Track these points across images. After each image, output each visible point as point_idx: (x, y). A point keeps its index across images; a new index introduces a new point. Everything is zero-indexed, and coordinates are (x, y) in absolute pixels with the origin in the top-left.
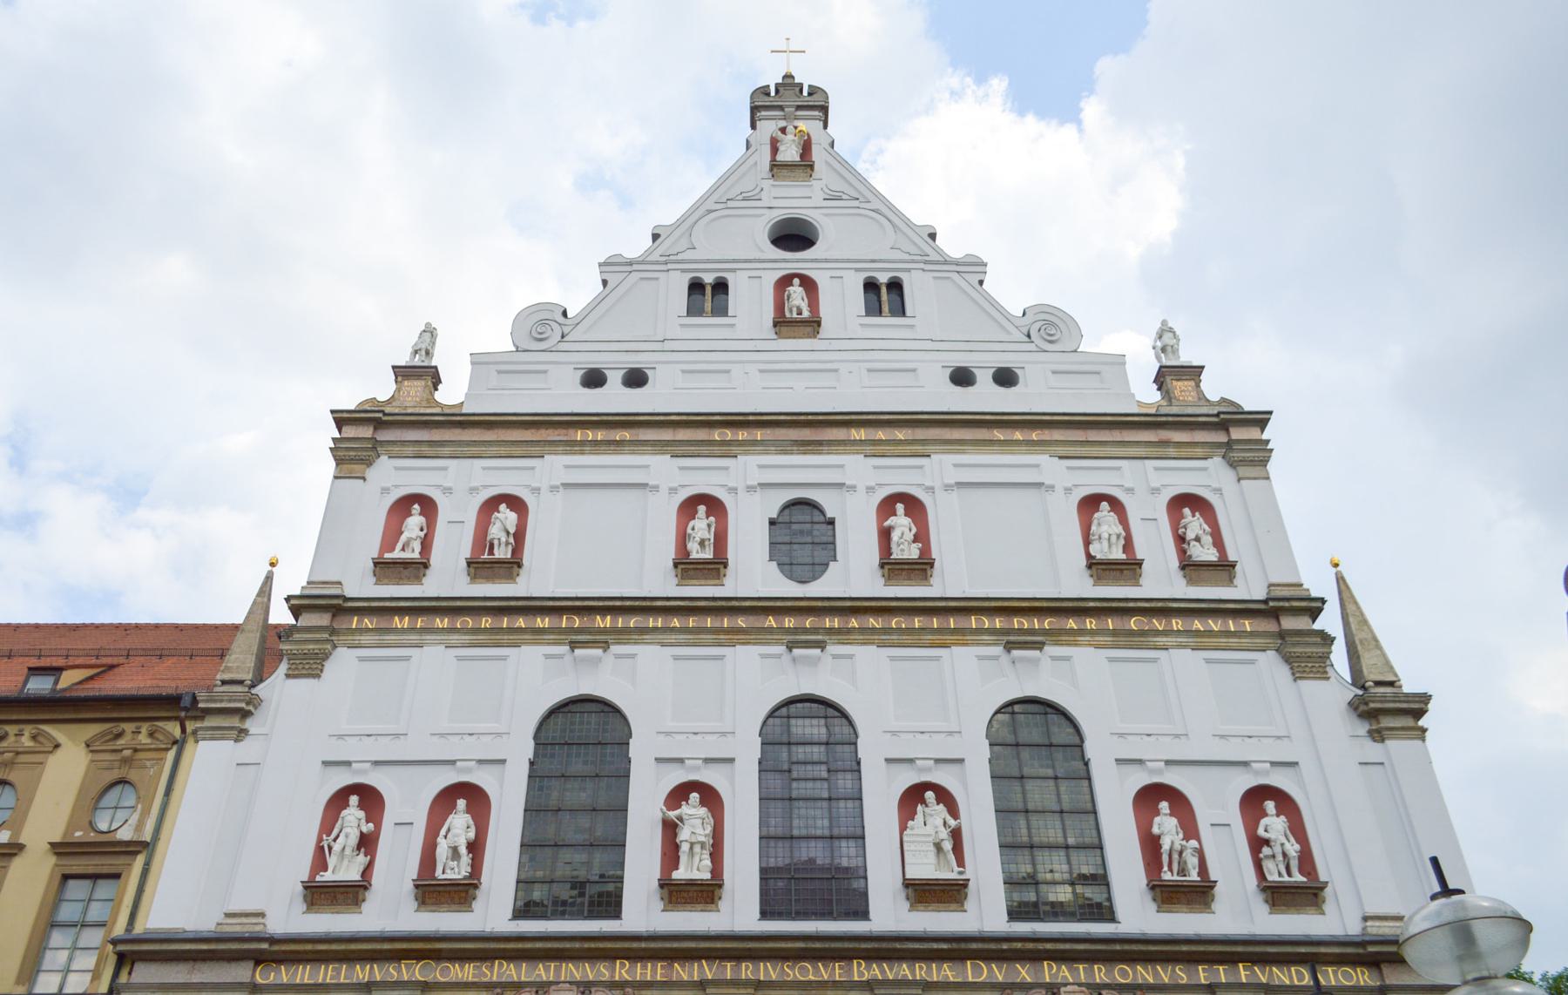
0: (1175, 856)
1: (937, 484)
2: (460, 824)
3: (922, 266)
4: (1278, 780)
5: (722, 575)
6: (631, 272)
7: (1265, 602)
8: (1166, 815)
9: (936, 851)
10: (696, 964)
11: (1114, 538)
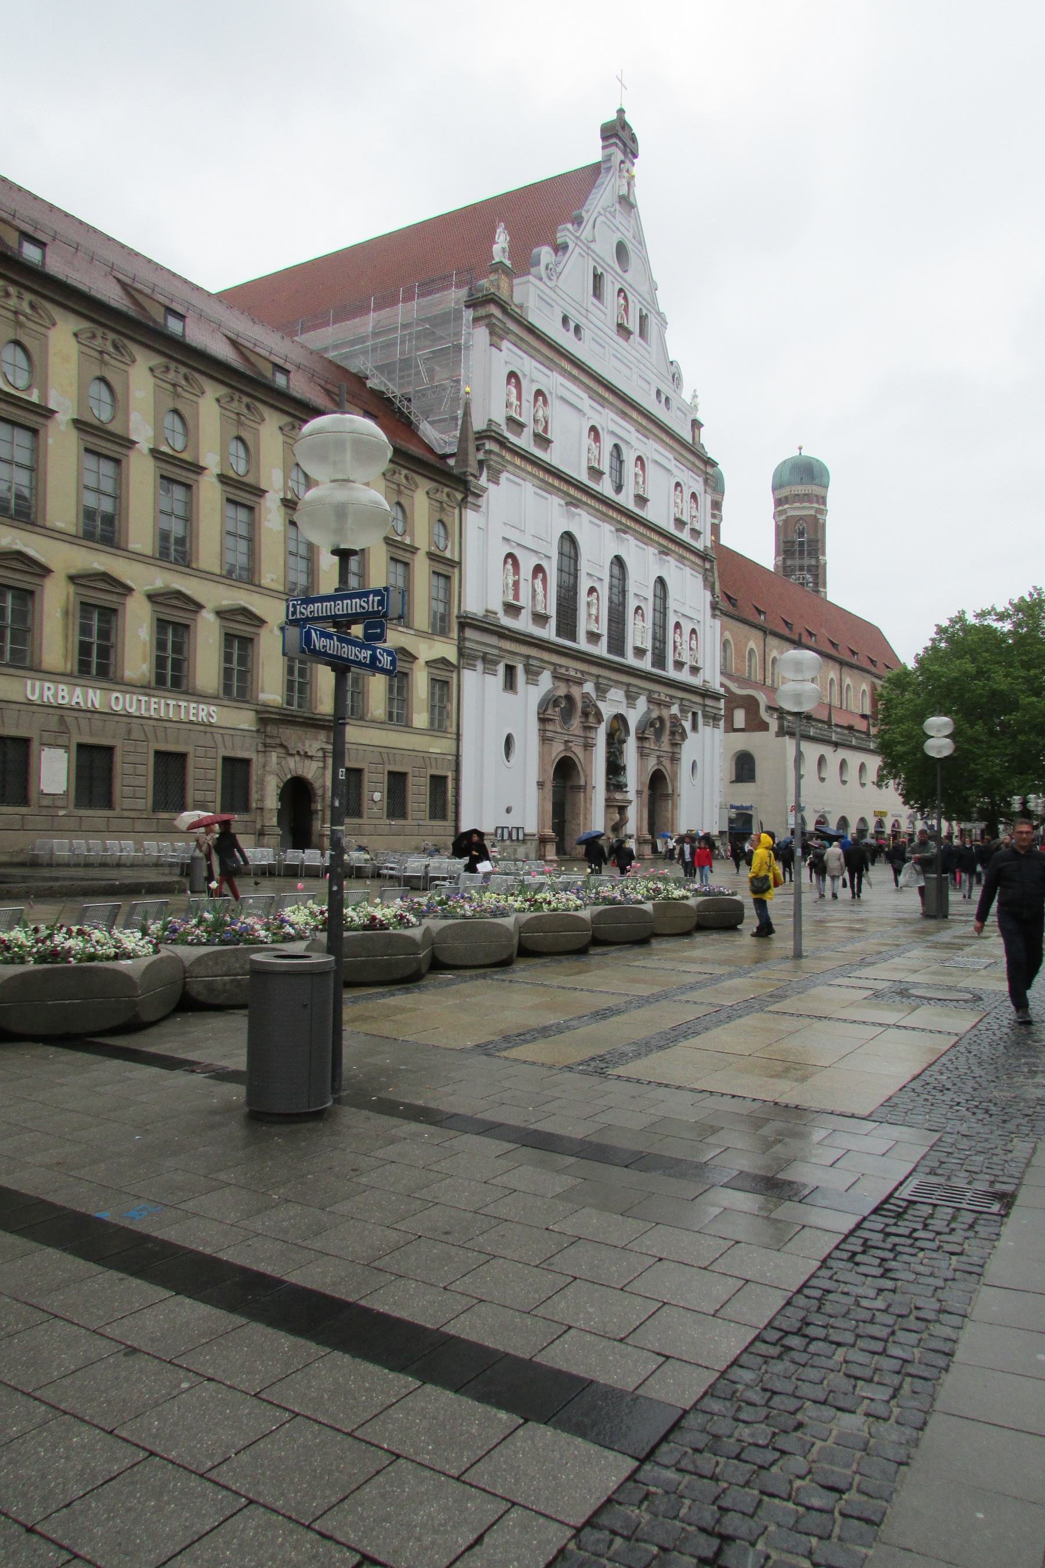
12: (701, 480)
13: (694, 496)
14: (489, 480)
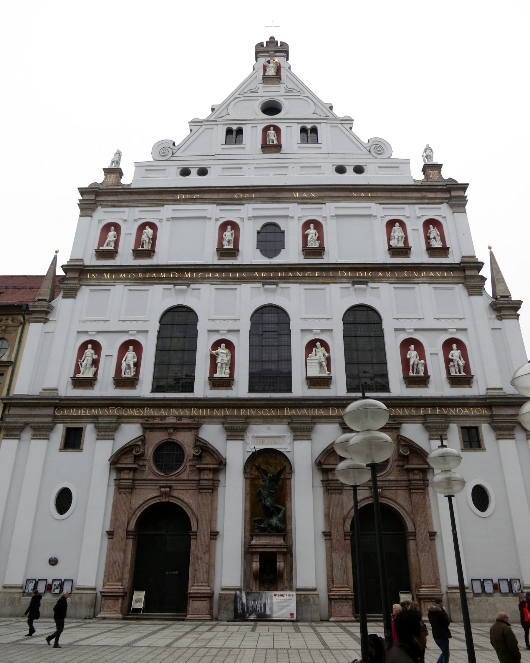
0: (415, 366)
1: (328, 216)
2: (130, 356)
3: (325, 121)
4: (459, 336)
5: (236, 255)
6: (202, 126)
7: (459, 264)
8: (413, 350)
9: (319, 366)
10: (223, 410)
11: (400, 238)
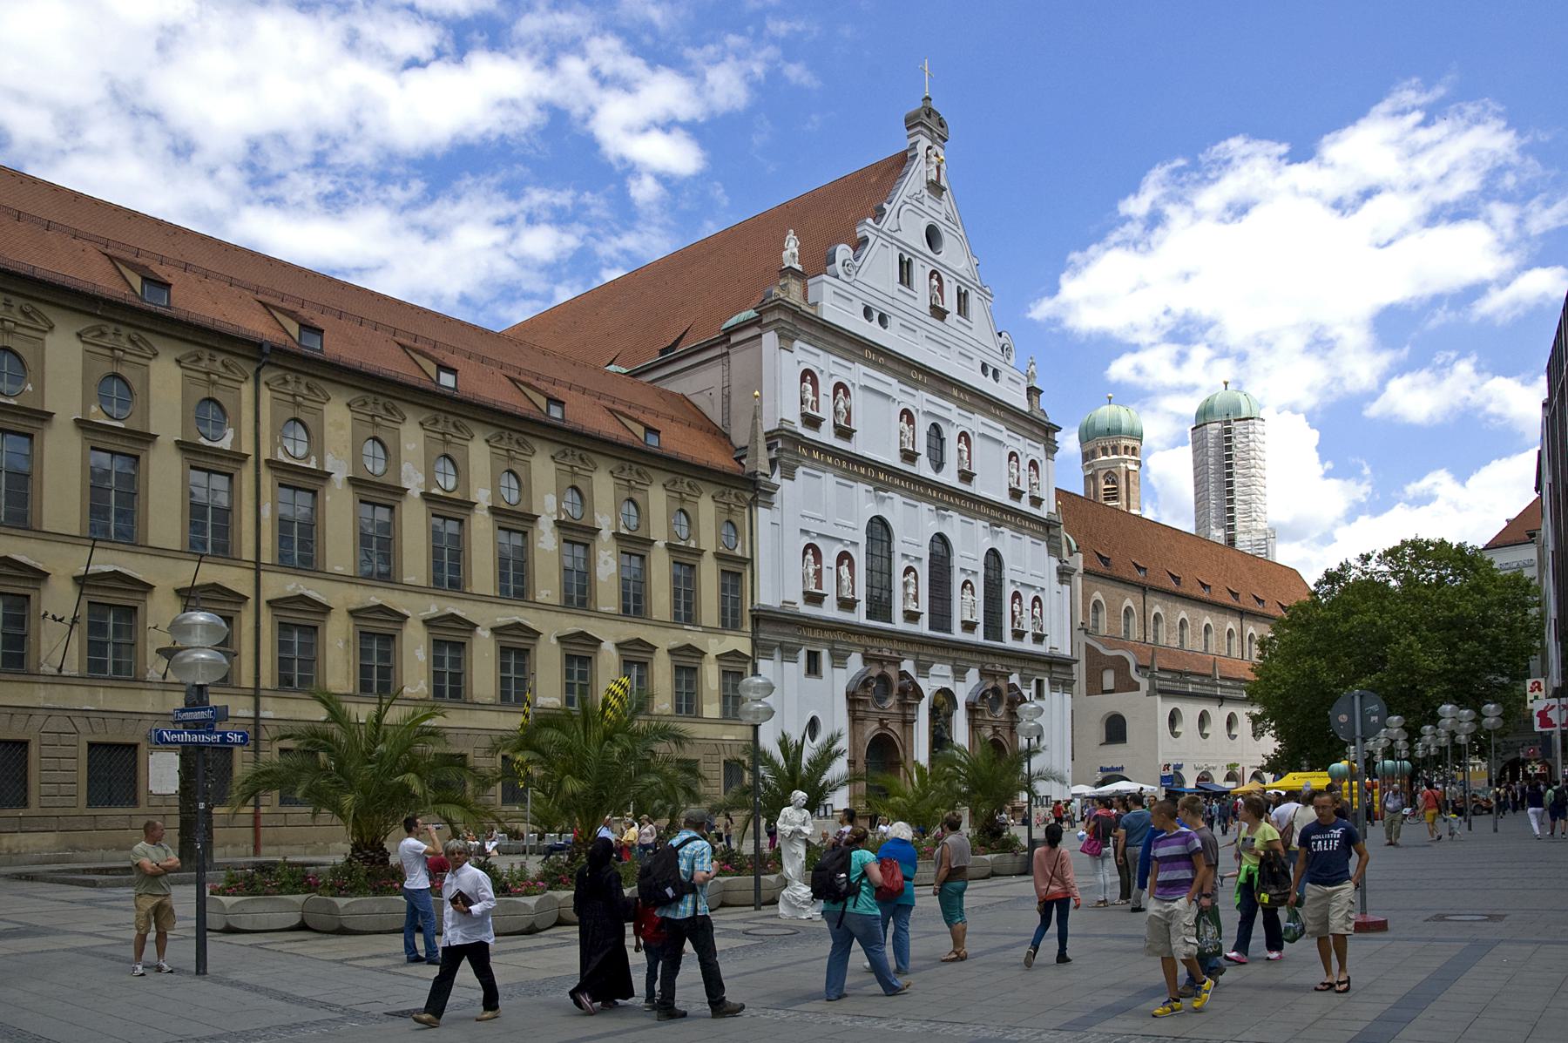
4: (1040, 595)
12: (1042, 447)
13: (1033, 464)
14: (782, 477)
